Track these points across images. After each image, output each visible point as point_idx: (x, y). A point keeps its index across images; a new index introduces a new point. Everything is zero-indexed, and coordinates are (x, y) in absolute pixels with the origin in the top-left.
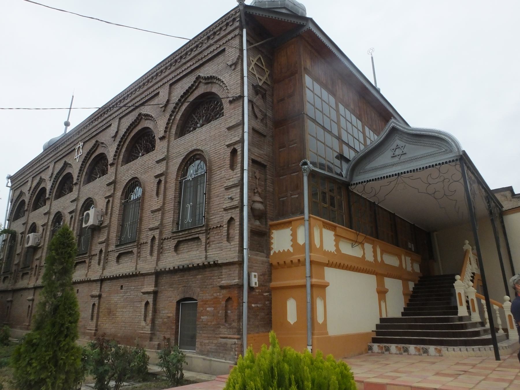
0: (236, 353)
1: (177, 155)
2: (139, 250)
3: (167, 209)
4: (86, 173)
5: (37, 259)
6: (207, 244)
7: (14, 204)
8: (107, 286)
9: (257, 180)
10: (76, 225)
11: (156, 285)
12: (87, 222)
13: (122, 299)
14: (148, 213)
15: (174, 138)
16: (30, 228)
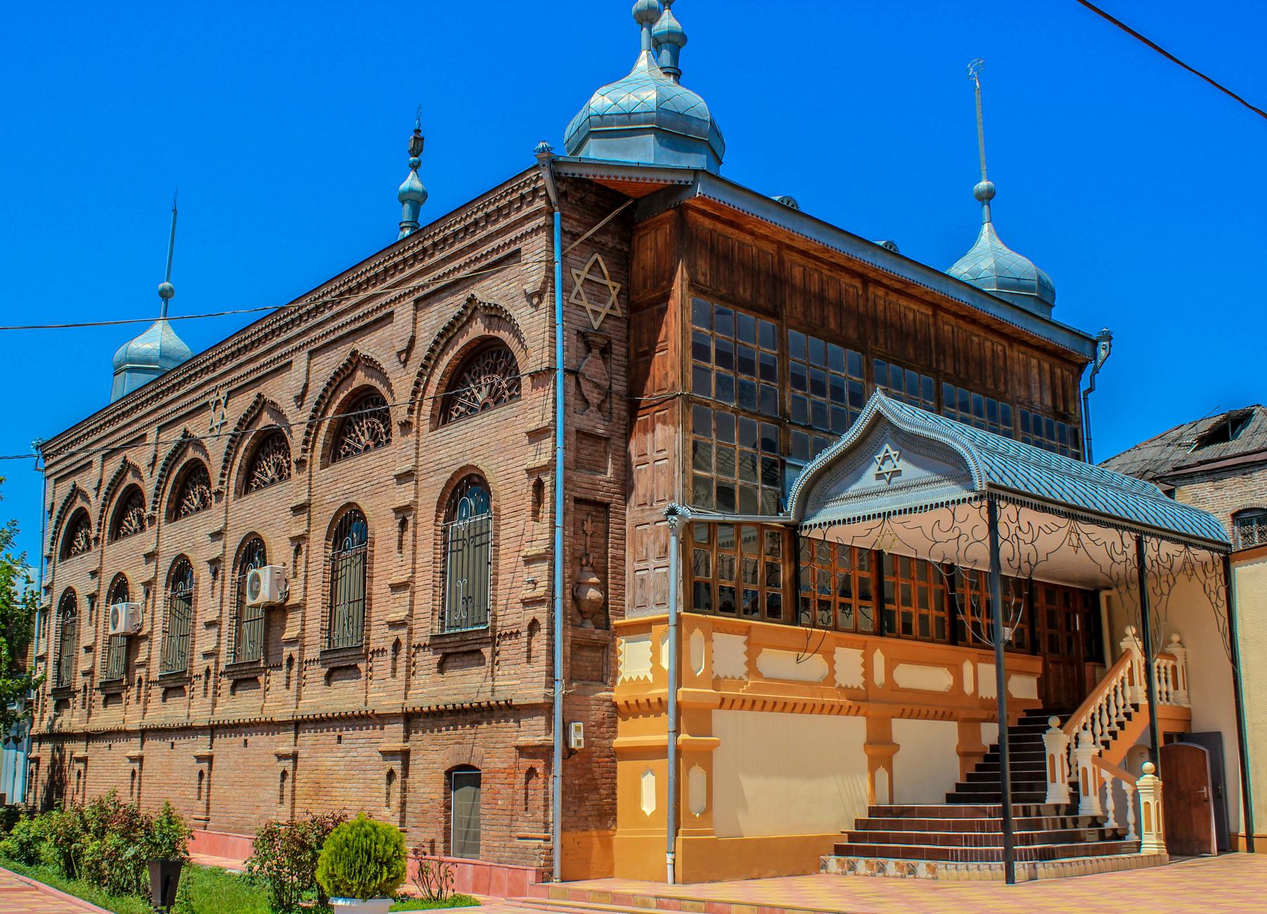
0: (542, 862)
1: (436, 468)
2: (370, 664)
3: (421, 584)
4: (240, 467)
5: (142, 665)
6: (495, 663)
7: (59, 517)
8: (307, 737)
9: (588, 538)
10: (227, 592)
11: (406, 739)
12: (255, 594)
13: (342, 763)
14: (383, 586)
15: (427, 427)
16: (112, 585)
